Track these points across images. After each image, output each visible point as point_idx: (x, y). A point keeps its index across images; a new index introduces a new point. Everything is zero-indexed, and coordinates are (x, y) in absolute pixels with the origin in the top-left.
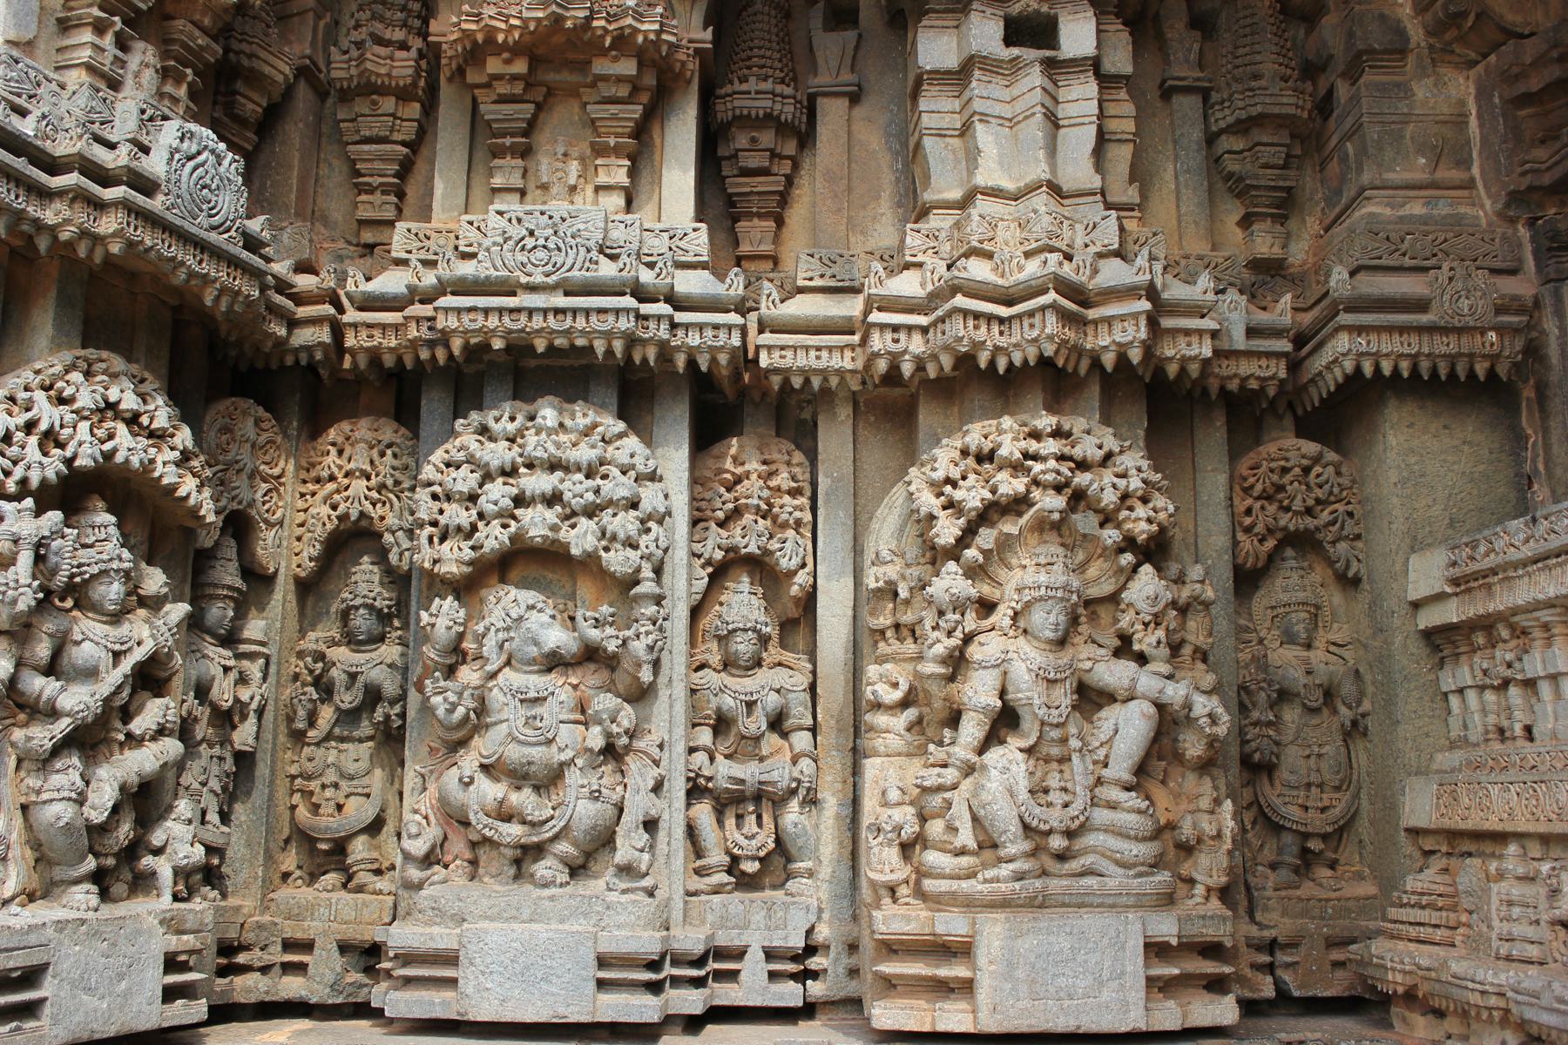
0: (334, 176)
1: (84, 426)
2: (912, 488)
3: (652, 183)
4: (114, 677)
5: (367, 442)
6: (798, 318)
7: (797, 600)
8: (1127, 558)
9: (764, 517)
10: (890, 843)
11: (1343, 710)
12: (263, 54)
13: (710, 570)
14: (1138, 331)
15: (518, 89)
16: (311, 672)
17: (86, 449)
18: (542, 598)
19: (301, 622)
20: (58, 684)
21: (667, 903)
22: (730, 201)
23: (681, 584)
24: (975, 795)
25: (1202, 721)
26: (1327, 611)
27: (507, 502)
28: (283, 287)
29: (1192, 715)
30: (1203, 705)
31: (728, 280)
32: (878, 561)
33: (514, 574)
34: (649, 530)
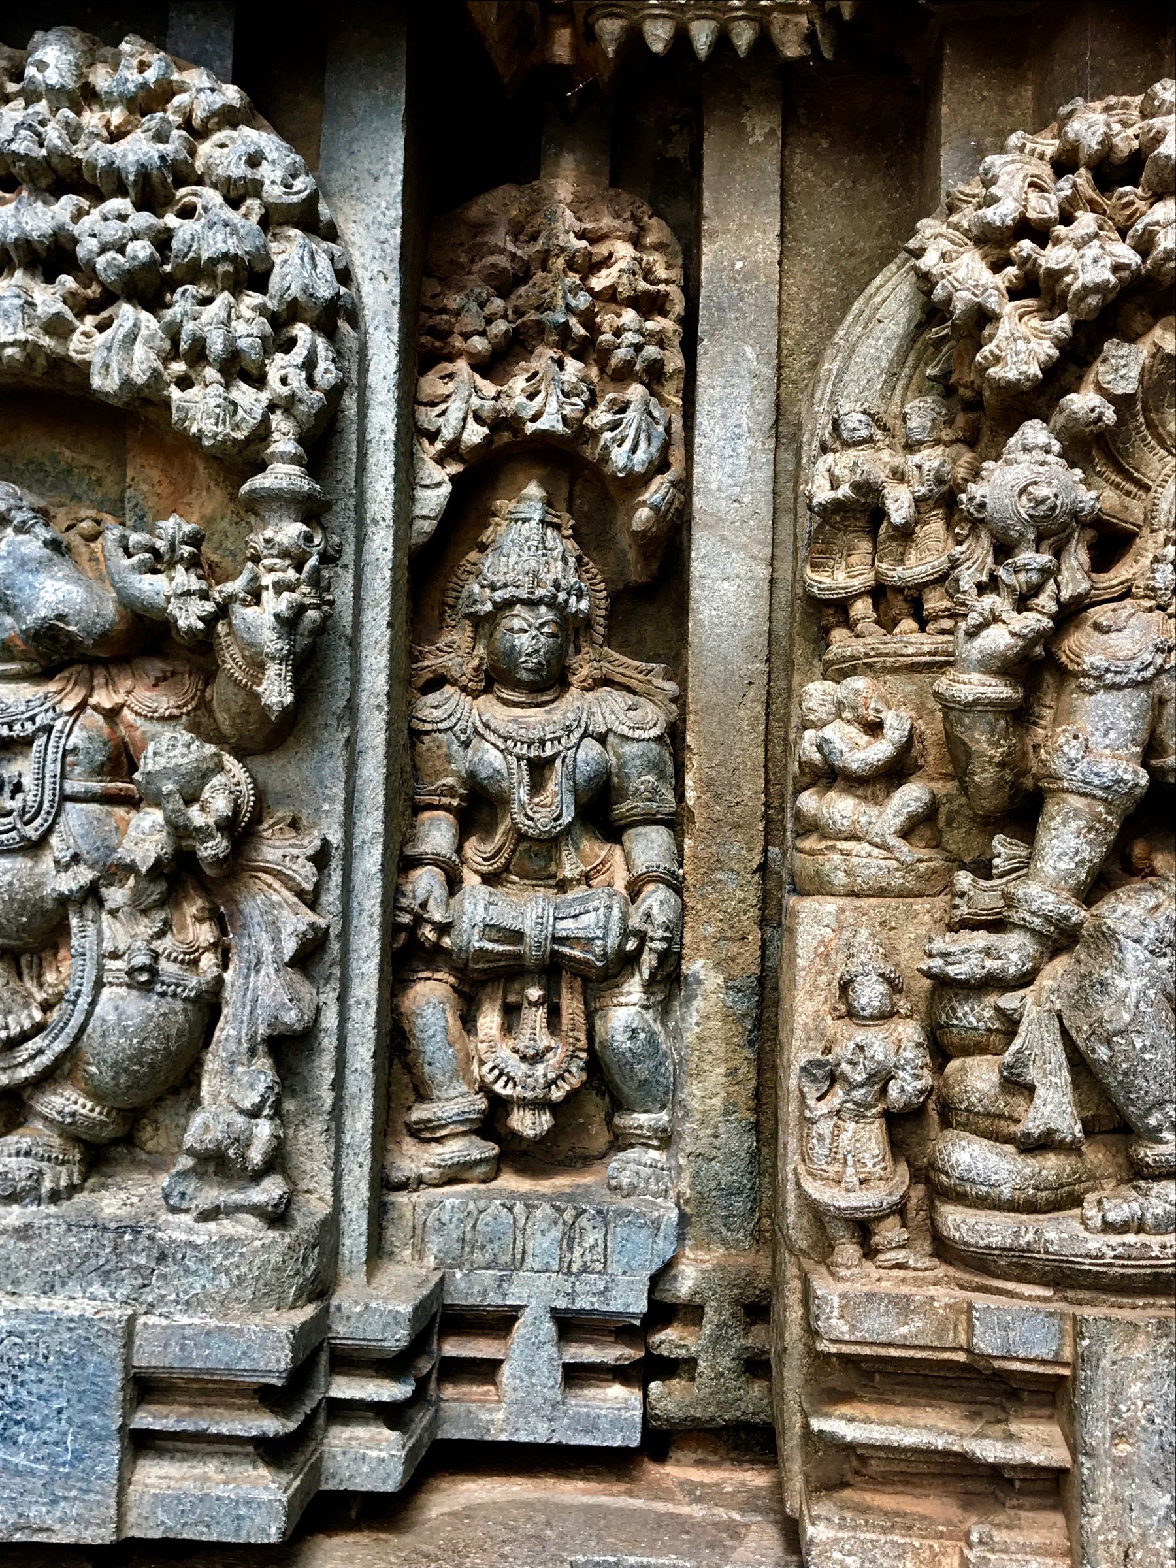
2: (930, 261)
9: (578, 356)
10: (860, 1112)
13: (455, 468)
21: (331, 1226)
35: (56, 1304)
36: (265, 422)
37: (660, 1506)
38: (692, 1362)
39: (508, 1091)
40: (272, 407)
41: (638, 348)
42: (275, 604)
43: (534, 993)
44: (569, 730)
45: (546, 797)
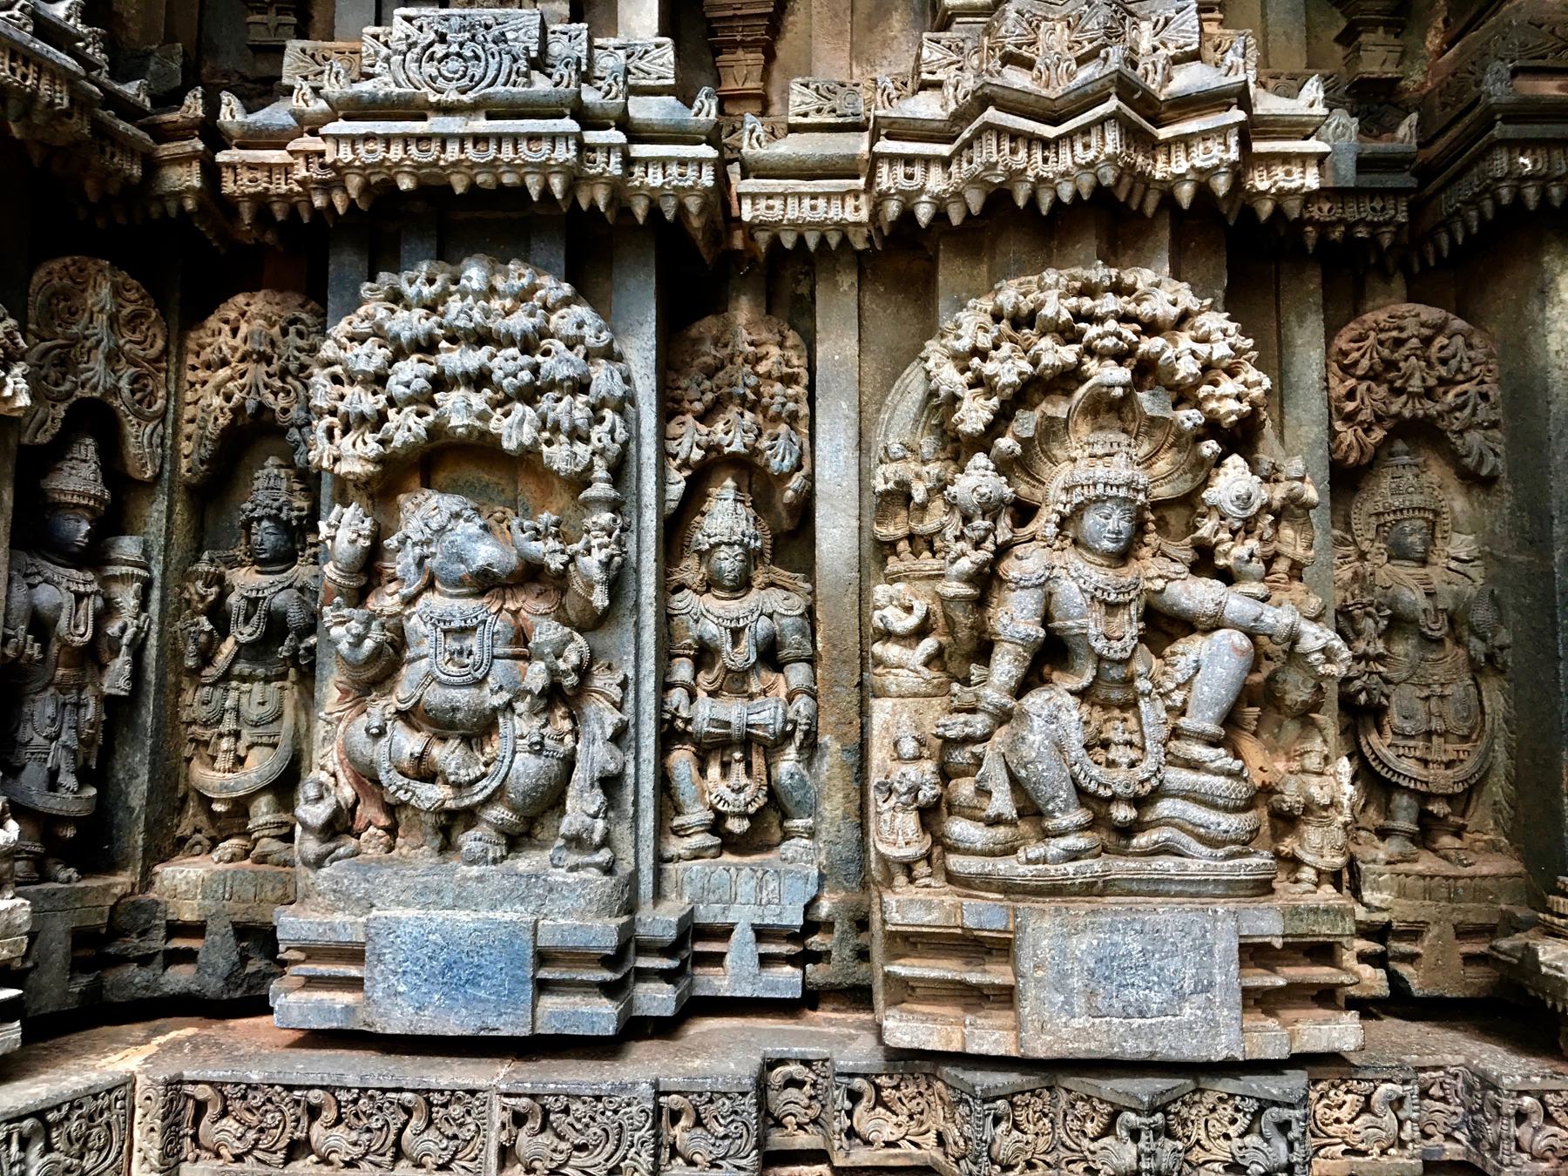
2: (930, 365)
5: (266, 318)
6: (789, 158)
7: (790, 507)
8: (1210, 447)
9: (751, 410)
11: (1475, 643)
13: (687, 473)
14: (1227, 149)
21: (634, 877)
24: (1013, 748)
25: (1313, 658)
26: (1447, 518)
29: (1299, 649)
30: (1315, 637)
31: (697, 104)
32: (888, 457)
33: (441, 477)
34: (601, 420)
35: (497, 915)
36: (591, 461)
37: (812, 1029)
38: (829, 953)
39: (725, 808)
40: (593, 454)
41: (783, 405)
42: (599, 555)
43: (738, 755)
44: (752, 612)
45: (741, 648)
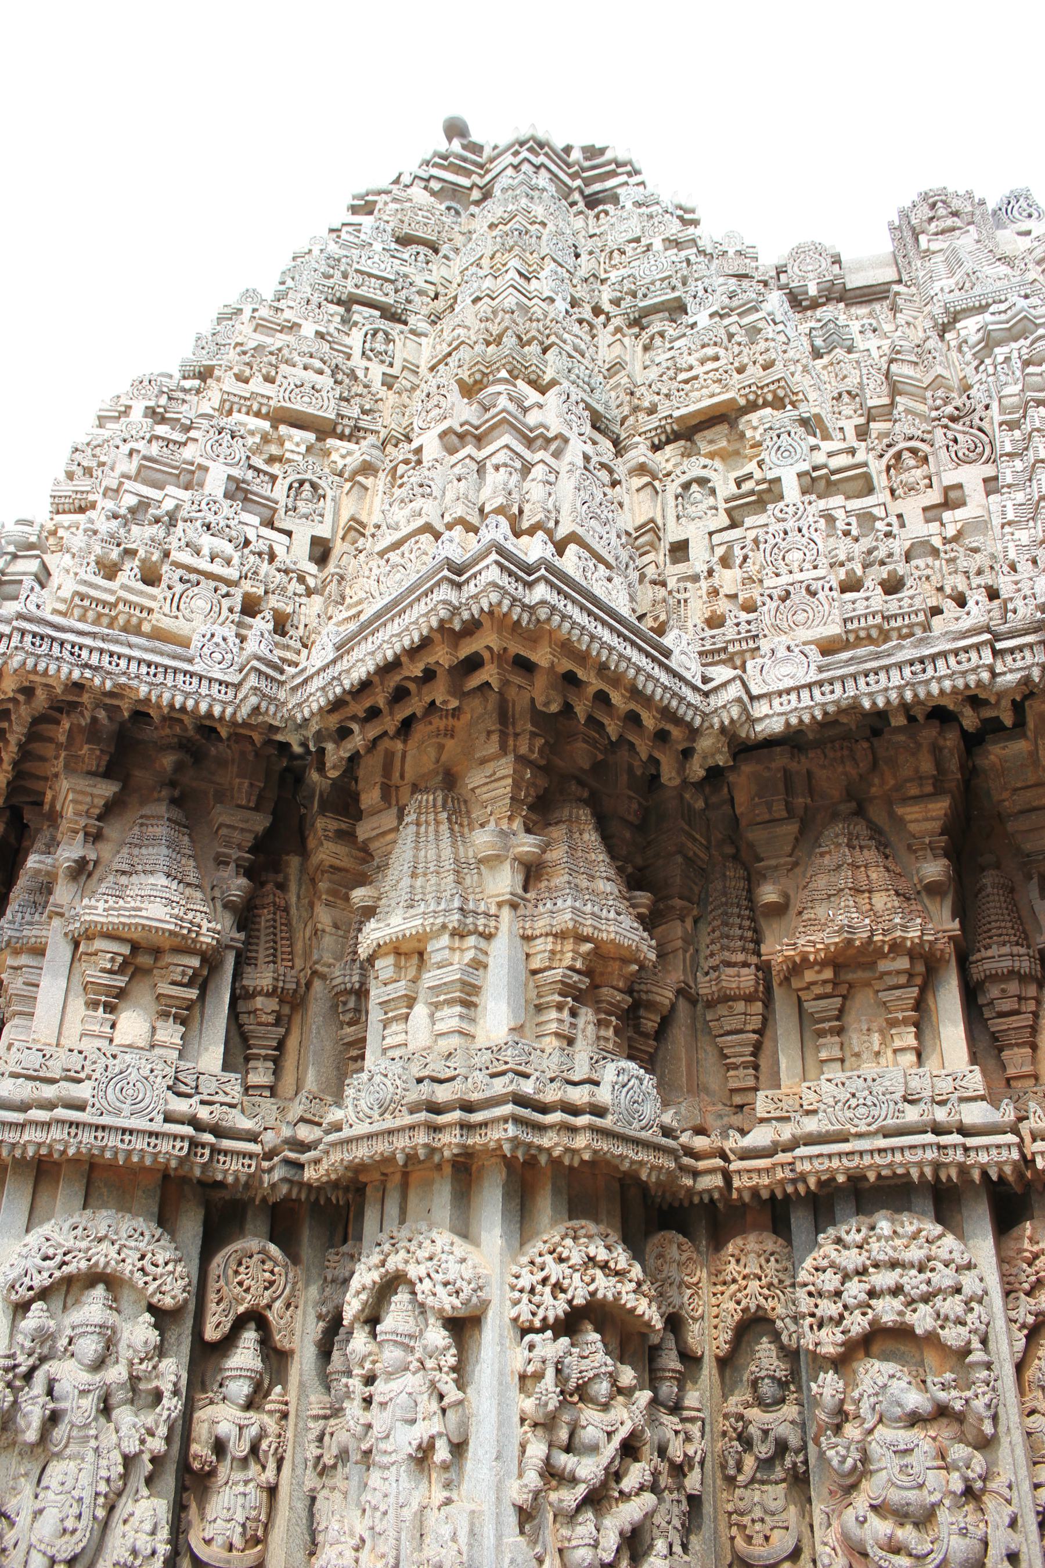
0: (709, 1059)
1: (577, 1276)
3: (934, 1038)
4: (611, 1449)
12: (655, 989)
13: (1025, 1332)
15: (829, 989)
16: (735, 1429)
17: (580, 1292)
18: (900, 1367)
19: (723, 1389)
20: (576, 1459)
22: (994, 1037)
23: (1004, 1348)
27: (863, 1296)
28: (690, 1152)
33: (875, 1348)
34: (972, 1309)
